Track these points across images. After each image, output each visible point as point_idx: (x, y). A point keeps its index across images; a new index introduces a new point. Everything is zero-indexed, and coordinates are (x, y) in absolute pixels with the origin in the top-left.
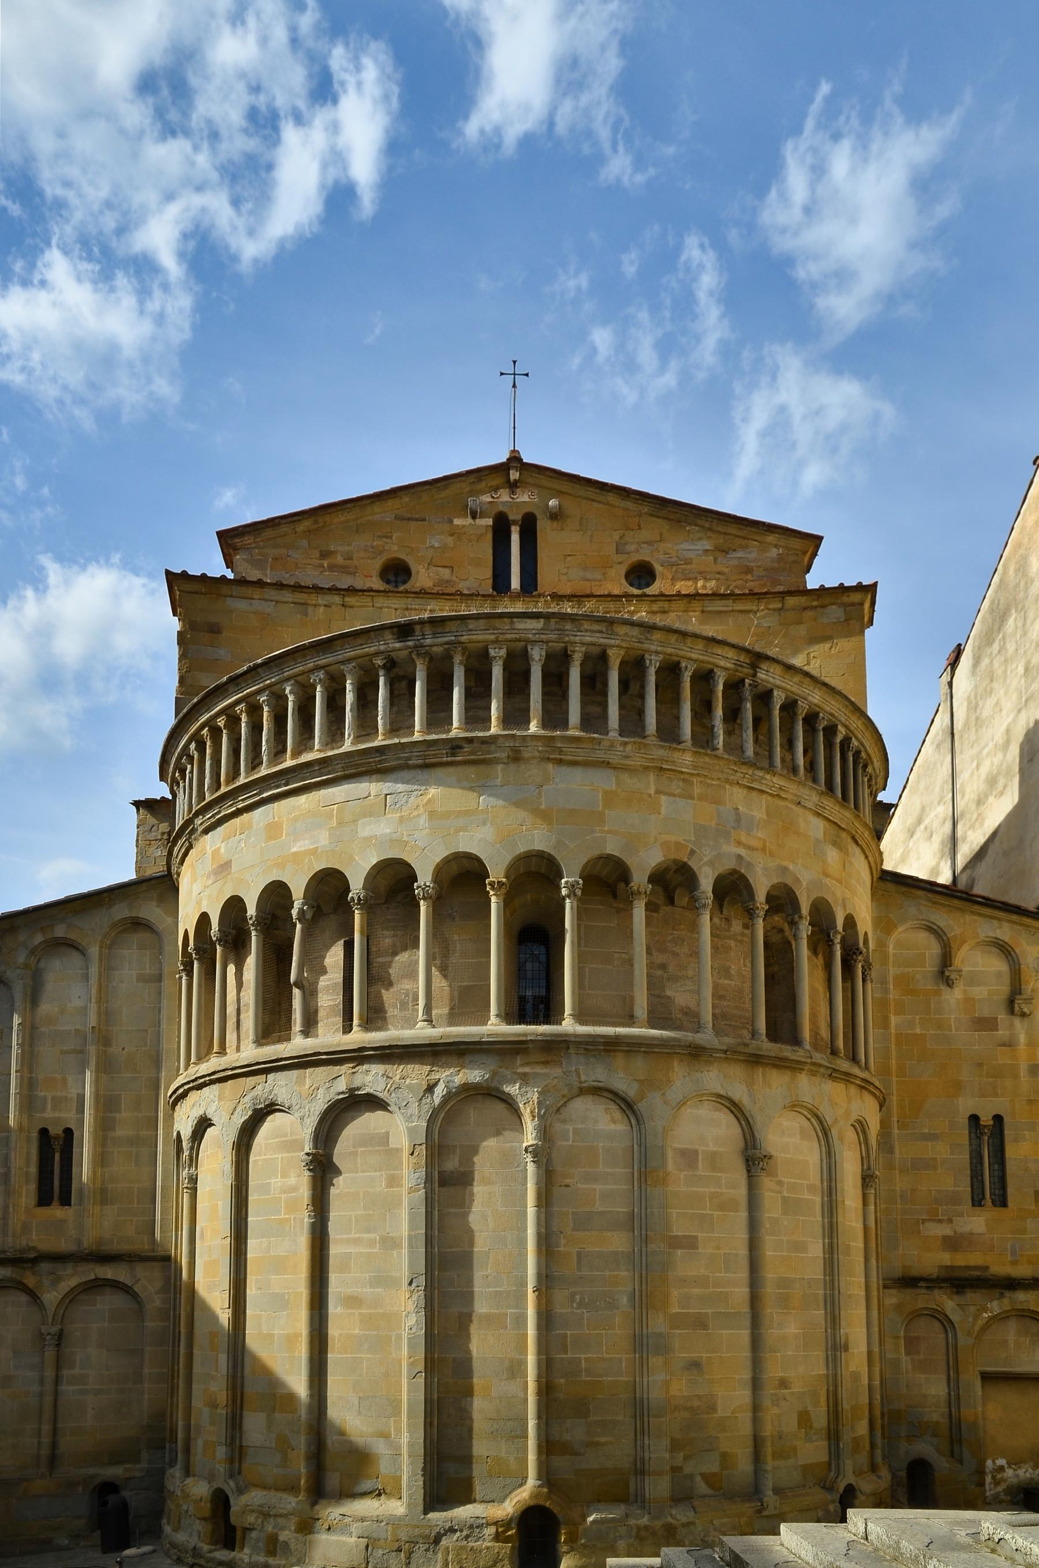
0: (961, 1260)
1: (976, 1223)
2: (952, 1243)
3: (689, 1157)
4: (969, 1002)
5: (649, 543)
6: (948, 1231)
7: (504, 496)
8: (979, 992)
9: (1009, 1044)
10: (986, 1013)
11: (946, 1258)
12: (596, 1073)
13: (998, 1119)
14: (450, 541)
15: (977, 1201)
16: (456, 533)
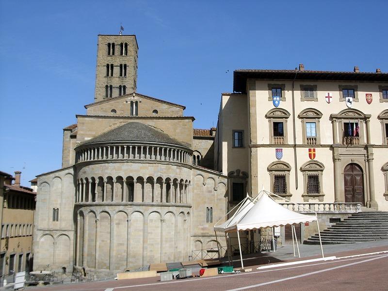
0: (204, 232)
1: (207, 225)
2: (203, 229)
3: (151, 221)
4: (208, 188)
5: (157, 106)
6: (202, 227)
7: (132, 97)
8: (209, 186)
9: (214, 195)
10: (210, 189)
11: (202, 232)
12: (138, 208)
13: (211, 208)
14: (123, 106)
15: (207, 222)
16: (124, 105)
